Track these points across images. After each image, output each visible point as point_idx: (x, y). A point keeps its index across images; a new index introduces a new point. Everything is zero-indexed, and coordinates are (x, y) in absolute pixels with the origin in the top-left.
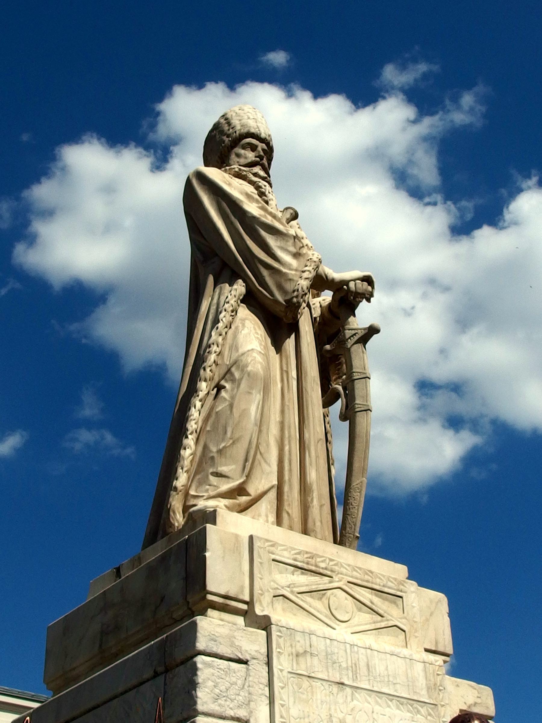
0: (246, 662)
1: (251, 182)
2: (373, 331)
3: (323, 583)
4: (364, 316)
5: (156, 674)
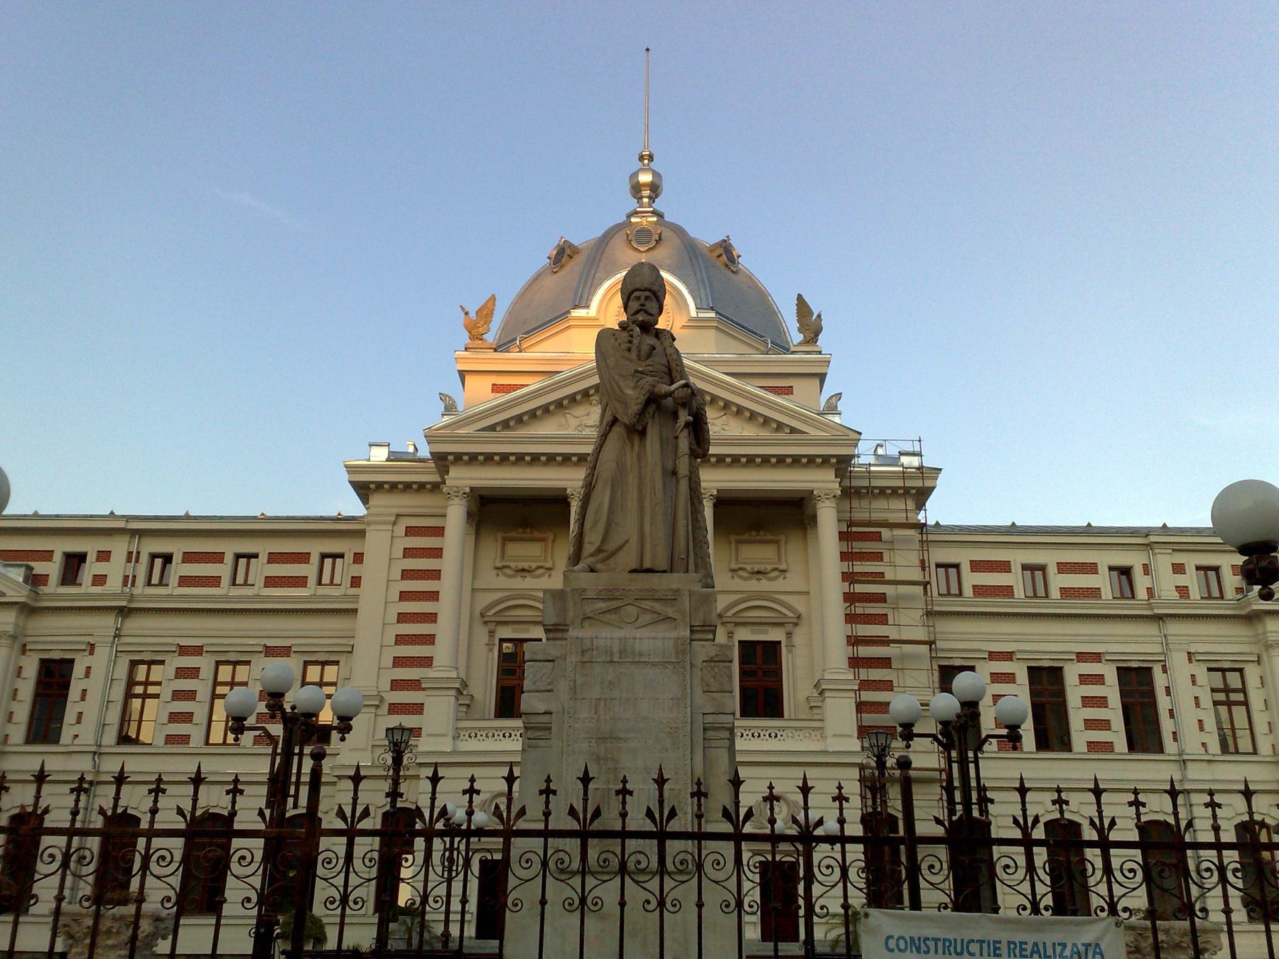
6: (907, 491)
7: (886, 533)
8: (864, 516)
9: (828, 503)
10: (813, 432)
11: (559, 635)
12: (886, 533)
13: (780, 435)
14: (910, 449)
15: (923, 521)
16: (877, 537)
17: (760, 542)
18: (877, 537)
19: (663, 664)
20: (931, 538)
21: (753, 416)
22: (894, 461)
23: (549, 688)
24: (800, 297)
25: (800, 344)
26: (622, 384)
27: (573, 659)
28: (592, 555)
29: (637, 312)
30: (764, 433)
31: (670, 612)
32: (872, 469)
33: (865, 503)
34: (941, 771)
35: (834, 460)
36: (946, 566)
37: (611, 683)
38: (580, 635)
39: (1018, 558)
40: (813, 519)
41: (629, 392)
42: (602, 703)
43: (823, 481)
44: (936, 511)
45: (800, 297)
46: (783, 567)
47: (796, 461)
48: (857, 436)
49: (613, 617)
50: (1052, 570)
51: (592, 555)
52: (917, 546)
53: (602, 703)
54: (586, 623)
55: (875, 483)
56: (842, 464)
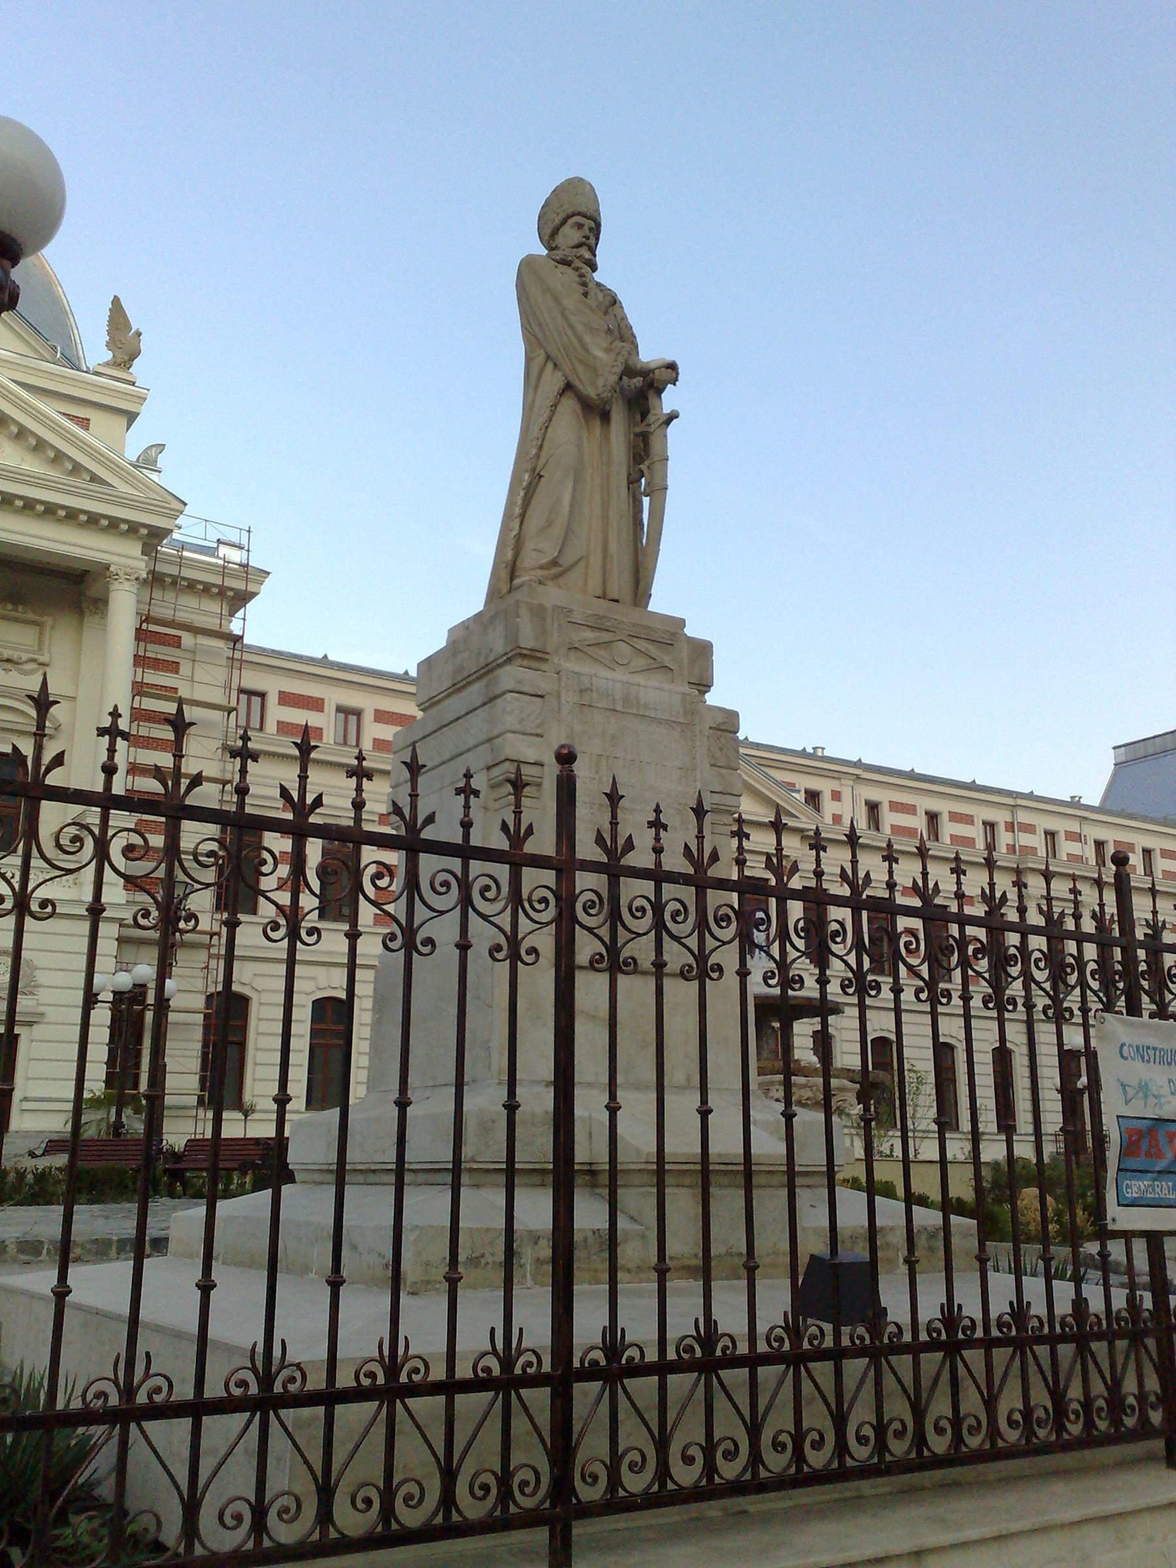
0: (542, 697)
1: (577, 269)
2: (673, 416)
3: (606, 636)
4: (670, 399)
5: (484, 704)
6: (222, 592)
7: (187, 639)
8: (166, 613)
9: (126, 586)
10: (123, 488)
11: (534, 664)
12: (187, 639)
13: (71, 480)
14: (236, 540)
15: (237, 631)
16: (176, 642)
17: (16, 620)
18: (176, 642)
19: (669, 723)
20: (246, 657)
21: (40, 446)
22: (211, 552)
23: (539, 731)
24: (116, 301)
25: (107, 364)
26: (587, 339)
27: (569, 698)
28: (542, 567)
29: (579, 246)
30: (53, 473)
31: (667, 659)
32: (185, 554)
33: (170, 596)
34: (212, 935)
35: (144, 531)
36: (250, 693)
37: (613, 738)
38: (577, 668)
39: (334, 696)
40: (101, 604)
41: (600, 354)
42: (604, 761)
43: (124, 556)
44: (258, 625)
45: (116, 301)
46: (42, 659)
47: (94, 521)
48: (179, 506)
49: (601, 653)
50: (368, 717)
51: (542, 567)
52: (224, 662)
53: (604, 761)
54: (572, 655)
55: (187, 573)
56: (153, 537)
